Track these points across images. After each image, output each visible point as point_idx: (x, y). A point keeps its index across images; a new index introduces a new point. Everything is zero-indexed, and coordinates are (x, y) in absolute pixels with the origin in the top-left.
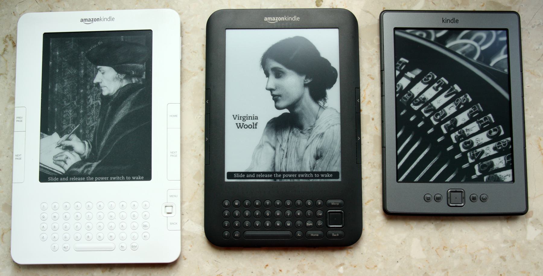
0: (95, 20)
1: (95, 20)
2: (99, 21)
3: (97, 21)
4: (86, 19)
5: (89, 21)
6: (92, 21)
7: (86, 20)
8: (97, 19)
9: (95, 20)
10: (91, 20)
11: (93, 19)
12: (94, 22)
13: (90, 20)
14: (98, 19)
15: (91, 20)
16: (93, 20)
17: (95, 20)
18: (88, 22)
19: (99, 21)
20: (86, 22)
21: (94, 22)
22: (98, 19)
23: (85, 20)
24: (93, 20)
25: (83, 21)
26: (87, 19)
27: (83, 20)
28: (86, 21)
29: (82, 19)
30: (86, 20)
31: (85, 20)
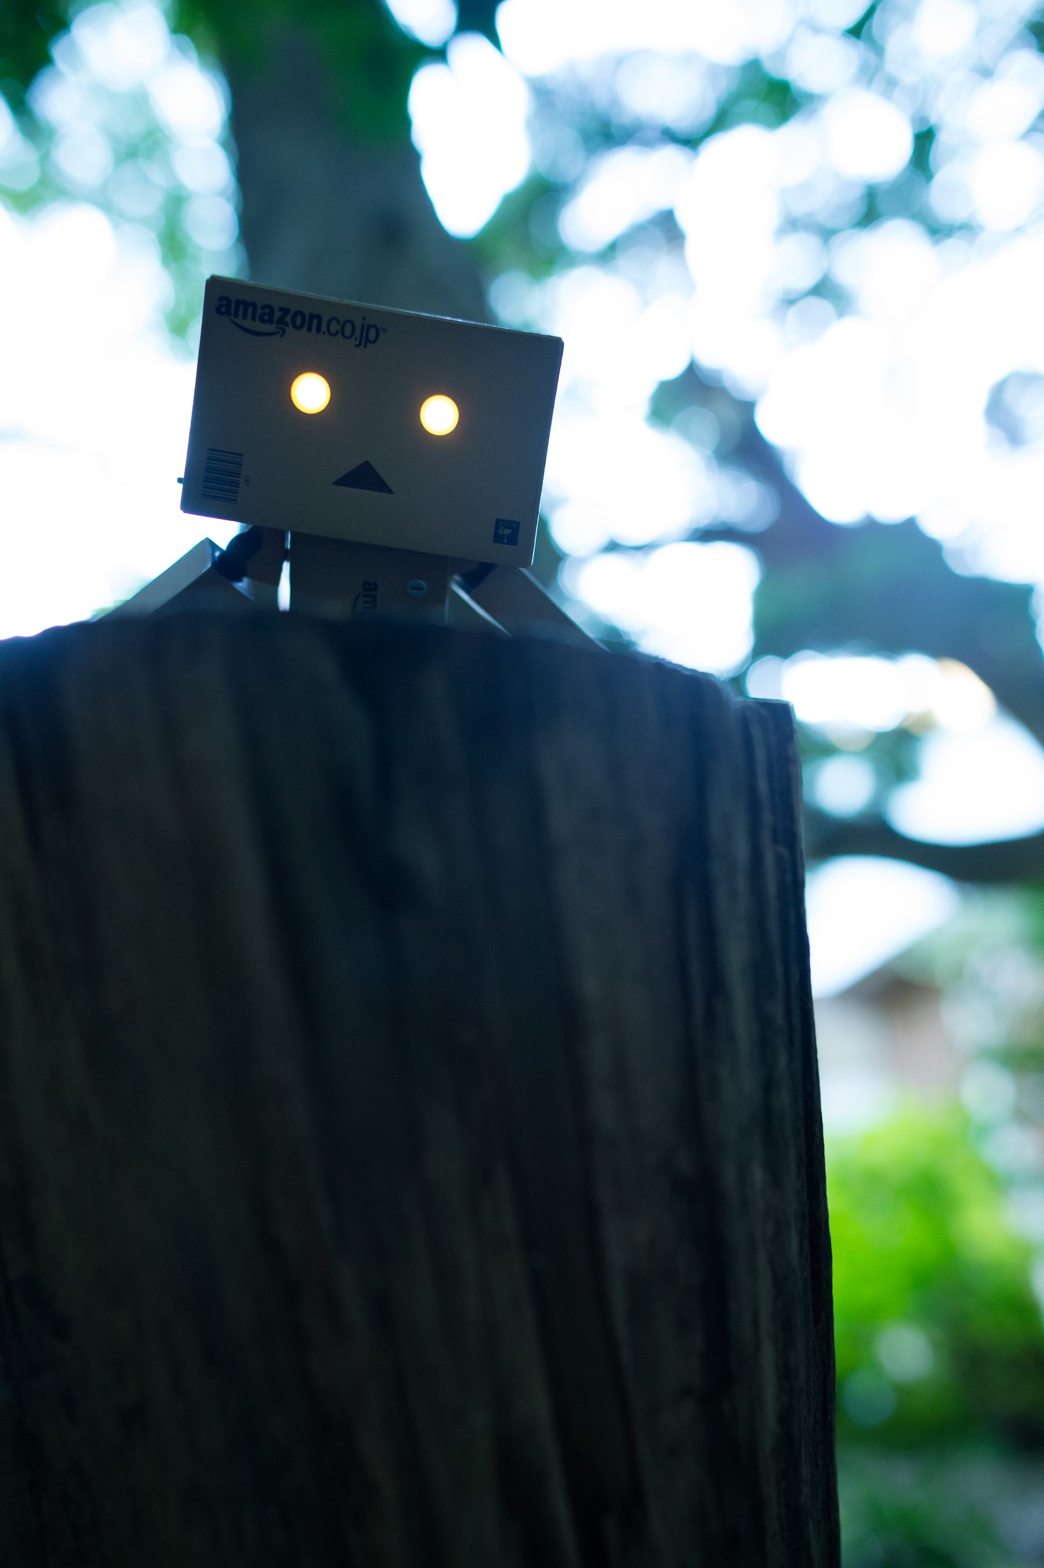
0: (298, 322)
1: (298, 322)
2: (318, 330)
3: (310, 329)
4: (246, 304)
5: (262, 320)
6: (281, 321)
7: (250, 309)
8: (312, 317)
9: (299, 318)
10: (277, 315)
11: (285, 311)
12: (290, 329)
13: (271, 314)
14: (315, 321)
15: (277, 315)
16: (288, 319)
17: (299, 318)
18: (258, 326)
19: (318, 330)
20: (248, 324)
21: (290, 329)
22: (315, 321)
23: (241, 308)
24: (288, 319)
25: (228, 313)
26: (254, 305)
27: (228, 306)
28: (245, 317)
29: (227, 299)
30: (250, 309)
31: (241, 308)
